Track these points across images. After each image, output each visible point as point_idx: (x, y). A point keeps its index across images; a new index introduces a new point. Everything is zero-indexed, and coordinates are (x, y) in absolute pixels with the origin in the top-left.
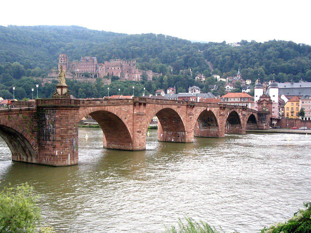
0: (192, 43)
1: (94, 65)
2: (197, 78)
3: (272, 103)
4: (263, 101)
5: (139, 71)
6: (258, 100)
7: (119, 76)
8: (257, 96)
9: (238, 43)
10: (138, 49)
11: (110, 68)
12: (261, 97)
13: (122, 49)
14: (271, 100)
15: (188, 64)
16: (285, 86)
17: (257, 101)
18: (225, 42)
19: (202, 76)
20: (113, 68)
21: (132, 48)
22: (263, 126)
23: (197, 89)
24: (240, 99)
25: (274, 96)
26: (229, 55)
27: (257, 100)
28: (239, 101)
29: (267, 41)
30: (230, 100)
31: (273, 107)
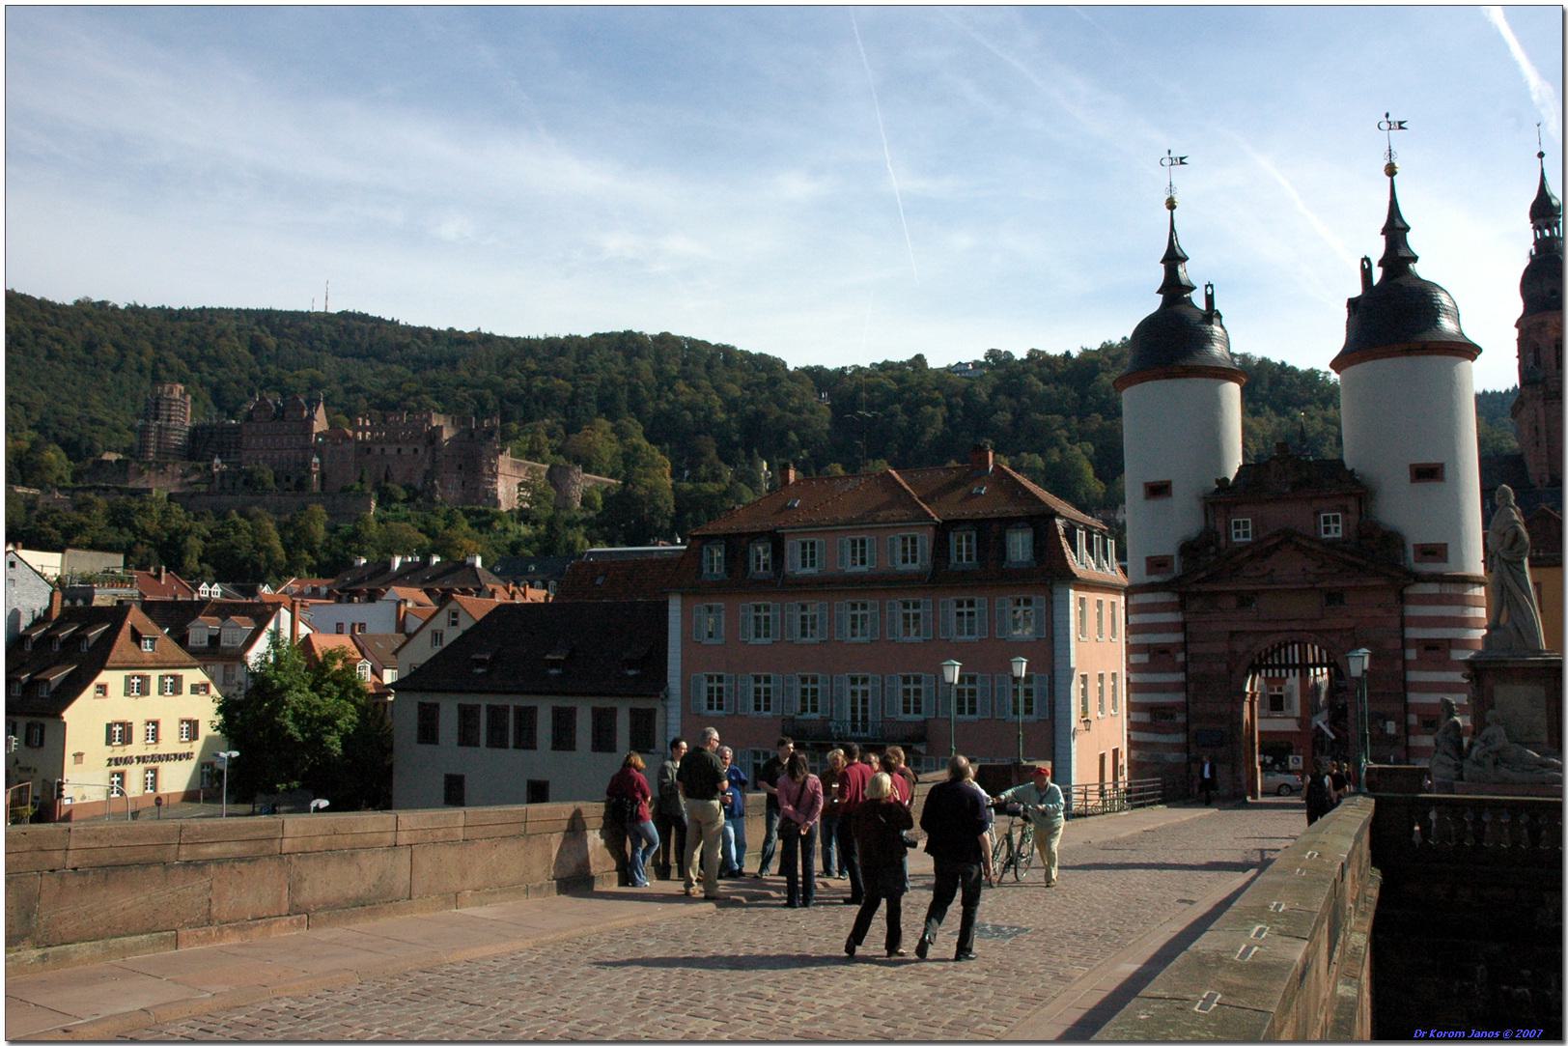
0: (791, 367)
4: (1260, 551)
5: (518, 466)
6: (1190, 549)
8: (1158, 490)
9: (976, 364)
11: (377, 449)
17: (1155, 564)
18: (919, 358)
20: (391, 450)
24: (925, 539)
26: (934, 403)
27: (1168, 547)
29: (1096, 347)
30: (809, 554)
31: (1430, 646)
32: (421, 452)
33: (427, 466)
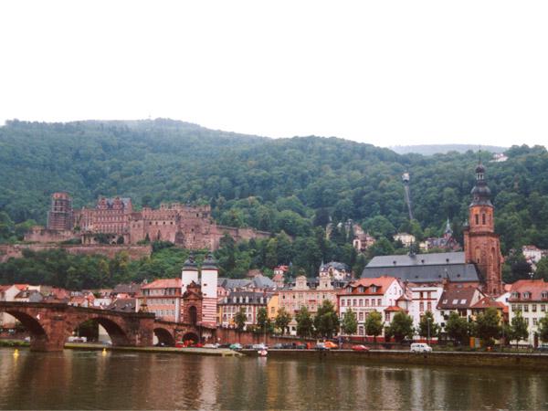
1: (123, 217)
2: (357, 242)
3: (201, 299)
7: (173, 240)
10: (264, 175)
11: (154, 223)
12: (188, 287)
13: (228, 175)
14: (201, 293)
15: (362, 209)
16: (448, 260)
19: (368, 239)
20: (160, 223)
21: (252, 173)
22: (135, 340)
23: (335, 268)
25: (205, 285)
26: (453, 186)
28: (162, 295)
32: (174, 223)
33: (177, 231)
